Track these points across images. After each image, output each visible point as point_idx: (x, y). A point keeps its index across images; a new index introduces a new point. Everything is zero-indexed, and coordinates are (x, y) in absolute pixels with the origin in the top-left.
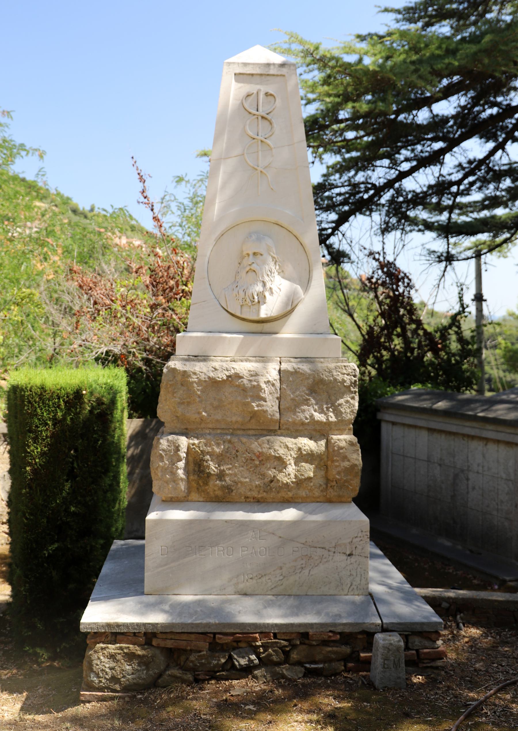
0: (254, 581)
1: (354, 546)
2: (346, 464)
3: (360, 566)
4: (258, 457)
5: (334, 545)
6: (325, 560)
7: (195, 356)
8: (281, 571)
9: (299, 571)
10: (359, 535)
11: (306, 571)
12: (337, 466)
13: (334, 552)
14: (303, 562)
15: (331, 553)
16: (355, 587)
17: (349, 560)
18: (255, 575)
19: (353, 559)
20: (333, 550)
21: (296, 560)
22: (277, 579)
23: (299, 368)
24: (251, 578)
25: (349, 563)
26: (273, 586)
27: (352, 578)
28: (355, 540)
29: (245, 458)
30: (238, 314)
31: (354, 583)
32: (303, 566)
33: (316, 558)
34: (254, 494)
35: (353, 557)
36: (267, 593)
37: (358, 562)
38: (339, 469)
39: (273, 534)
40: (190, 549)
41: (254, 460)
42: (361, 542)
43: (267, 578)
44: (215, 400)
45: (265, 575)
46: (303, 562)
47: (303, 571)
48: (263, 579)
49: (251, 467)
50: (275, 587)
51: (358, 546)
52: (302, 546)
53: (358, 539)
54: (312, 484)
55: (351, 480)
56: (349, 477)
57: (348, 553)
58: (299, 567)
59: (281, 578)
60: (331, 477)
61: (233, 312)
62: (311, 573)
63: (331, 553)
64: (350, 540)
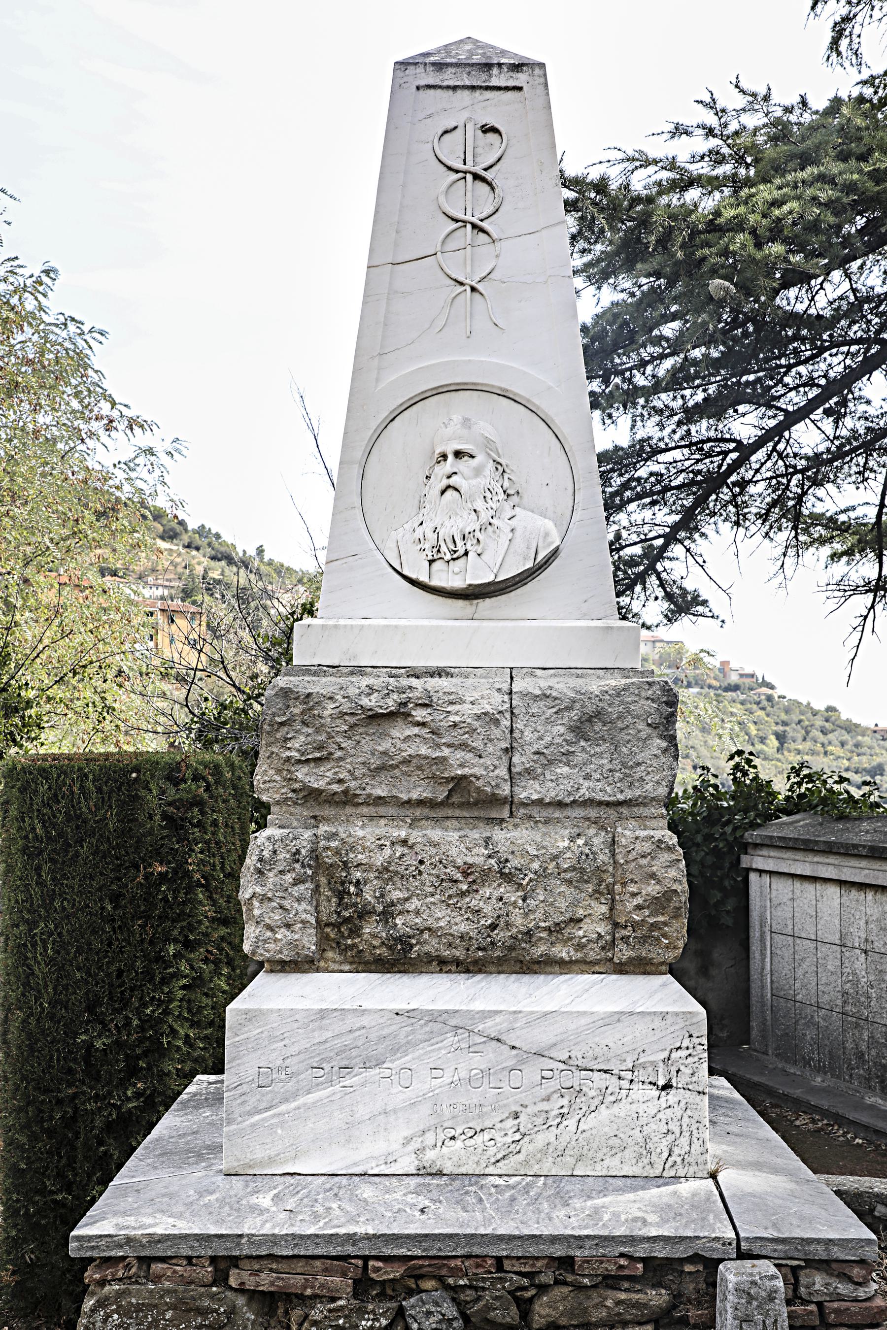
0: (458, 1144)
1: (674, 1069)
2: (652, 889)
3: (689, 1112)
4: (466, 874)
5: (630, 1066)
6: (613, 1098)
7: (334, 667)
8: (516, 1122)
9: (555, 1123)
10: (684, 1045)
11: (571, 1122)
12: (634, 895)
13: (632, 1081)
14: (565, 1102)
15: (625, 1084)
16: (679, 1160)
17: (663, 1099)
18: (460, 1131)
19: (672, 1097)
20: (629, 1075)
21: (548, 1099)
22: (509, 1139)
23: (551, 688)
24: (453, 1138)
25: (664, 1105)
26: (499, 1156)
27: (670, 1138)
28: (675, 1055)
29: (438, 876)
30: (424, 578)
31: (676, 1150)
32: (565, 1110)
33: (592, 1093)
34: (458, 953)
35: (673, 1092)
36: (487, 1171)
37: (682, 1104)
38: (639, 900)
39: (498, 1040)
40: (321, 1072)
41: (456, 881)
42: (690, 1060)
43: (487, 1136)
44: (373, 754)
45: (482, 1130)
46: (565, 1102)
47: (565, 1123)
48: (479, 1139)
49: (450, 897)
50: (504, 1157)
51: (682, 1068)
52: (562, 1066)
53: (683, 1053)
54: (581, 933)
55: (665, 924)
56: (661, 919)
57: (661, 1082)
58: (556, 1112)
59: (518, 1136)
60: (622, 920)
61: (413, 576)
62: (582, 1126)
63: (625, 1084)
64: (665, 1054)
